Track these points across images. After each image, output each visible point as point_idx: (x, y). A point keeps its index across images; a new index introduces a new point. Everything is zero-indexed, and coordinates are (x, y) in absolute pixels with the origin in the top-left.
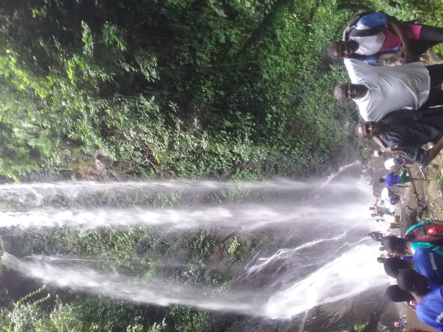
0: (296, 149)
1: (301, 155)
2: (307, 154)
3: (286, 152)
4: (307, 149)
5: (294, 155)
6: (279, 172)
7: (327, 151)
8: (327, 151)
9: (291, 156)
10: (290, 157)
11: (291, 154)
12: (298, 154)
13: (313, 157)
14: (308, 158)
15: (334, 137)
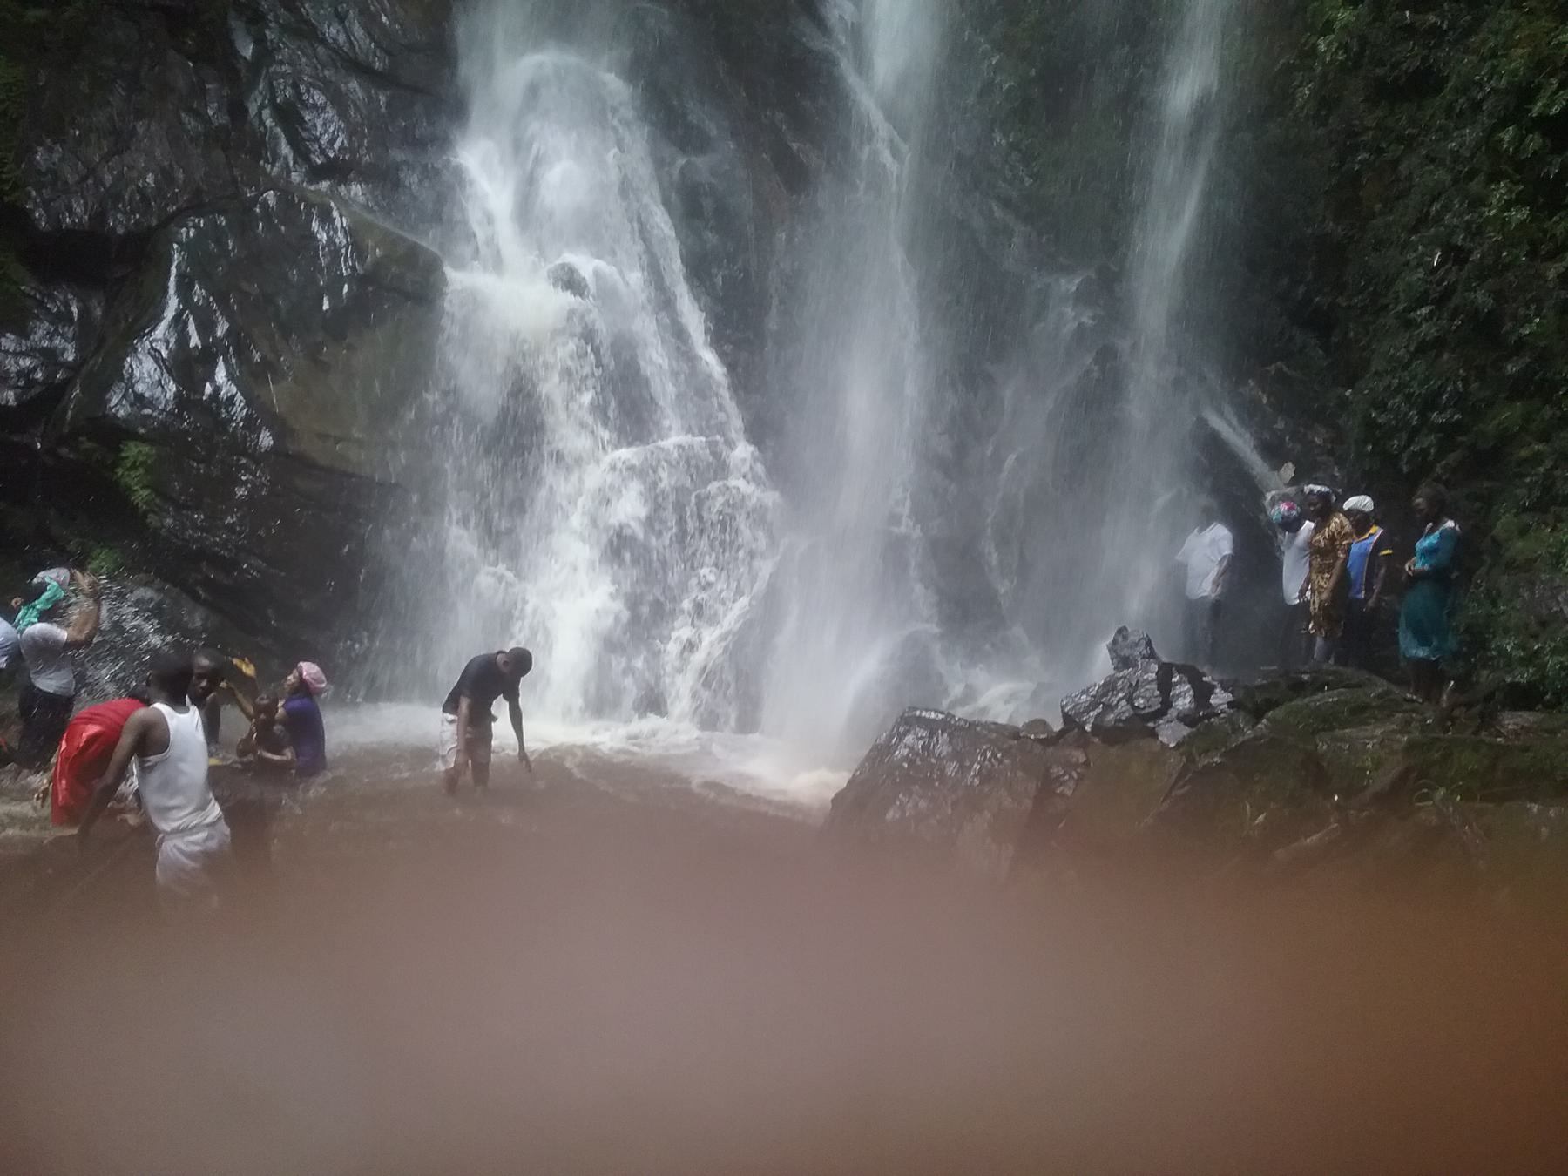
0: (1518, 215)
1: (1455, 255)
2: (1455, 300)
3: (1508, 135)
4: (1499, 296)
5: (1478, 202)
6: (1379, 113)
7: (1453, 458)
8: (1453, 458)
9: (1475, 186)
10: (1471, 175)
11: (1494, 178)
12: (1475, 232)
13: (1422, 348)
14: (1424, 311)
15: (1539, 507)
